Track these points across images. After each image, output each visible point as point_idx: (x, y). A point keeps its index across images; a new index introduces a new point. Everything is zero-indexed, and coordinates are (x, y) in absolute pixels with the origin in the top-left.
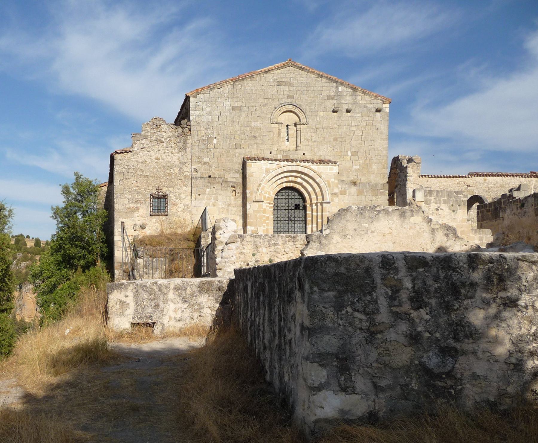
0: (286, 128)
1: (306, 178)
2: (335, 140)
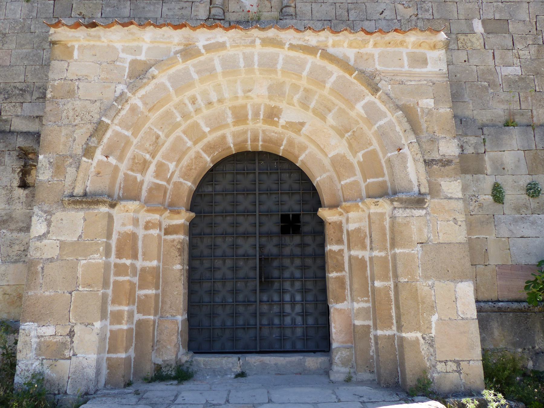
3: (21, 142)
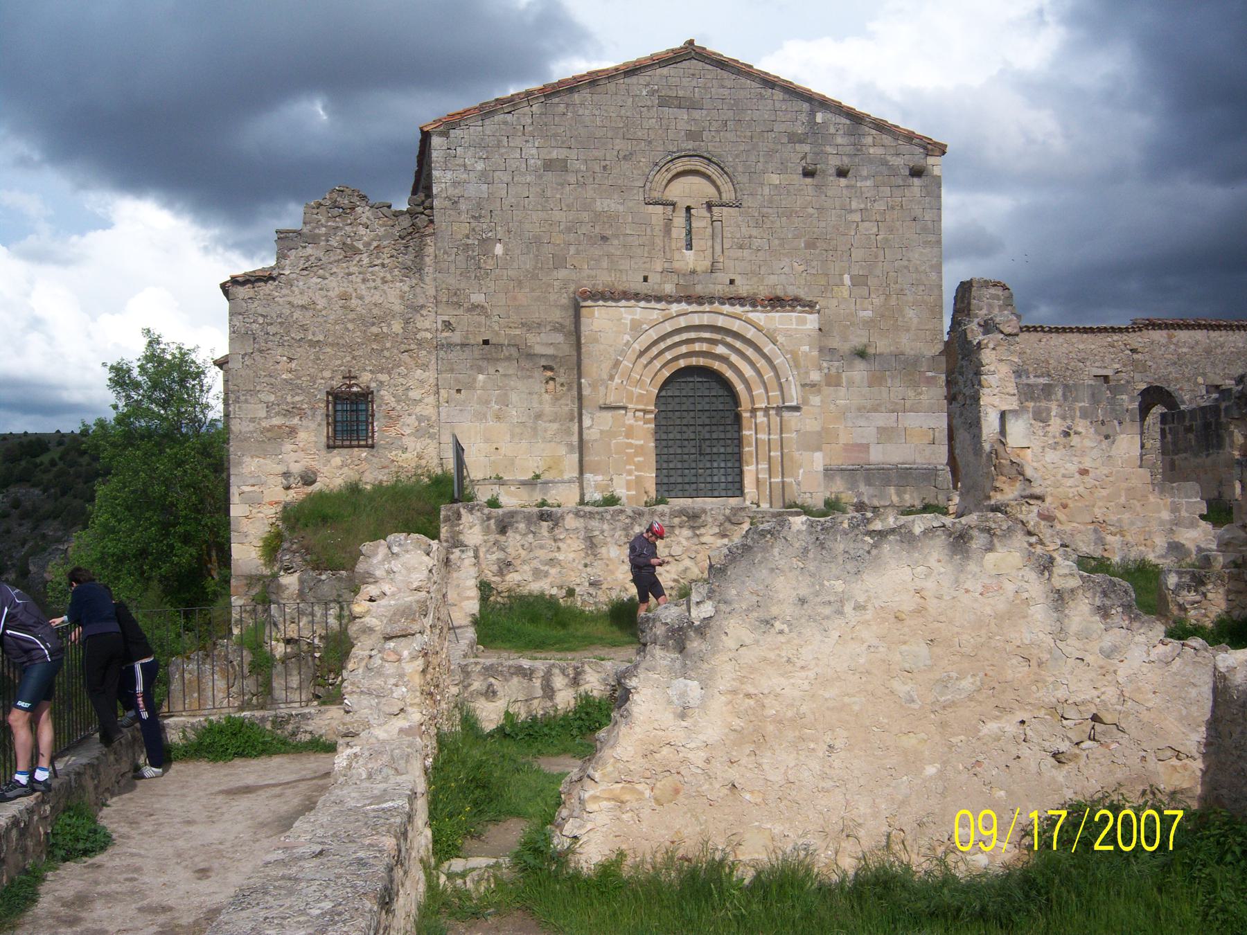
0: (683, 213)
1: (738, 344)
2: (810, 245)
3: (543, 362)
